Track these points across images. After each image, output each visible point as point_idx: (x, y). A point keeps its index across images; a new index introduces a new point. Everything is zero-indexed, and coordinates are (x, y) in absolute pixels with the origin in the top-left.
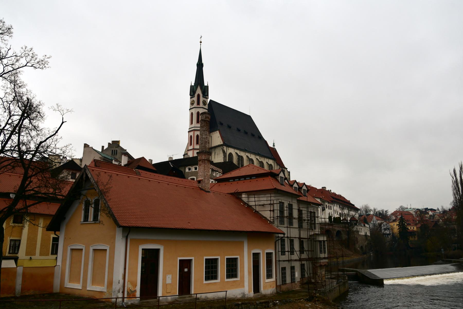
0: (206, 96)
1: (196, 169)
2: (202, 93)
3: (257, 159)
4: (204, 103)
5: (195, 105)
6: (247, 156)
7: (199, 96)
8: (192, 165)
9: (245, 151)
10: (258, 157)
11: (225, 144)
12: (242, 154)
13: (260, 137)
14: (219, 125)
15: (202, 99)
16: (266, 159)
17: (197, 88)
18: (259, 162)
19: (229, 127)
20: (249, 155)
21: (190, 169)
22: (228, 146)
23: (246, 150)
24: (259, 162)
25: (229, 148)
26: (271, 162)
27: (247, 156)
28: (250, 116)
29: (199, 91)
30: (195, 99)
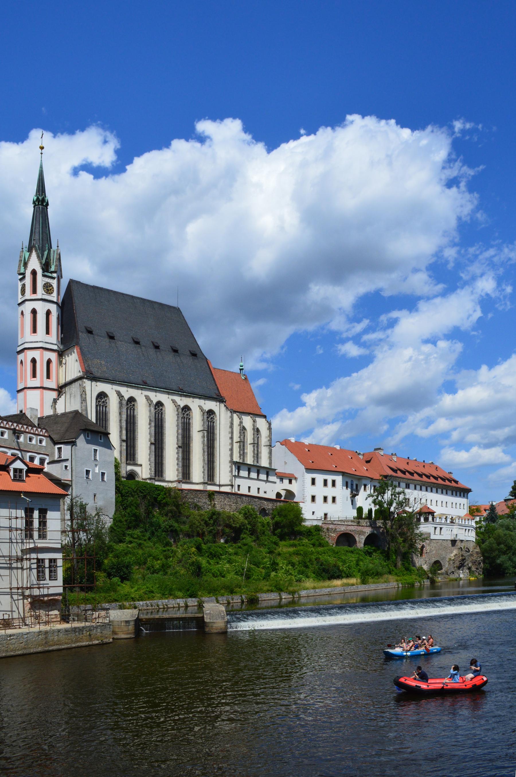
3: (174, 401)
5: (28, 294)
19: (112, 338)
23: (145, 383)
24: (177, 406)
28: (176, 311)
30: (28, 281)
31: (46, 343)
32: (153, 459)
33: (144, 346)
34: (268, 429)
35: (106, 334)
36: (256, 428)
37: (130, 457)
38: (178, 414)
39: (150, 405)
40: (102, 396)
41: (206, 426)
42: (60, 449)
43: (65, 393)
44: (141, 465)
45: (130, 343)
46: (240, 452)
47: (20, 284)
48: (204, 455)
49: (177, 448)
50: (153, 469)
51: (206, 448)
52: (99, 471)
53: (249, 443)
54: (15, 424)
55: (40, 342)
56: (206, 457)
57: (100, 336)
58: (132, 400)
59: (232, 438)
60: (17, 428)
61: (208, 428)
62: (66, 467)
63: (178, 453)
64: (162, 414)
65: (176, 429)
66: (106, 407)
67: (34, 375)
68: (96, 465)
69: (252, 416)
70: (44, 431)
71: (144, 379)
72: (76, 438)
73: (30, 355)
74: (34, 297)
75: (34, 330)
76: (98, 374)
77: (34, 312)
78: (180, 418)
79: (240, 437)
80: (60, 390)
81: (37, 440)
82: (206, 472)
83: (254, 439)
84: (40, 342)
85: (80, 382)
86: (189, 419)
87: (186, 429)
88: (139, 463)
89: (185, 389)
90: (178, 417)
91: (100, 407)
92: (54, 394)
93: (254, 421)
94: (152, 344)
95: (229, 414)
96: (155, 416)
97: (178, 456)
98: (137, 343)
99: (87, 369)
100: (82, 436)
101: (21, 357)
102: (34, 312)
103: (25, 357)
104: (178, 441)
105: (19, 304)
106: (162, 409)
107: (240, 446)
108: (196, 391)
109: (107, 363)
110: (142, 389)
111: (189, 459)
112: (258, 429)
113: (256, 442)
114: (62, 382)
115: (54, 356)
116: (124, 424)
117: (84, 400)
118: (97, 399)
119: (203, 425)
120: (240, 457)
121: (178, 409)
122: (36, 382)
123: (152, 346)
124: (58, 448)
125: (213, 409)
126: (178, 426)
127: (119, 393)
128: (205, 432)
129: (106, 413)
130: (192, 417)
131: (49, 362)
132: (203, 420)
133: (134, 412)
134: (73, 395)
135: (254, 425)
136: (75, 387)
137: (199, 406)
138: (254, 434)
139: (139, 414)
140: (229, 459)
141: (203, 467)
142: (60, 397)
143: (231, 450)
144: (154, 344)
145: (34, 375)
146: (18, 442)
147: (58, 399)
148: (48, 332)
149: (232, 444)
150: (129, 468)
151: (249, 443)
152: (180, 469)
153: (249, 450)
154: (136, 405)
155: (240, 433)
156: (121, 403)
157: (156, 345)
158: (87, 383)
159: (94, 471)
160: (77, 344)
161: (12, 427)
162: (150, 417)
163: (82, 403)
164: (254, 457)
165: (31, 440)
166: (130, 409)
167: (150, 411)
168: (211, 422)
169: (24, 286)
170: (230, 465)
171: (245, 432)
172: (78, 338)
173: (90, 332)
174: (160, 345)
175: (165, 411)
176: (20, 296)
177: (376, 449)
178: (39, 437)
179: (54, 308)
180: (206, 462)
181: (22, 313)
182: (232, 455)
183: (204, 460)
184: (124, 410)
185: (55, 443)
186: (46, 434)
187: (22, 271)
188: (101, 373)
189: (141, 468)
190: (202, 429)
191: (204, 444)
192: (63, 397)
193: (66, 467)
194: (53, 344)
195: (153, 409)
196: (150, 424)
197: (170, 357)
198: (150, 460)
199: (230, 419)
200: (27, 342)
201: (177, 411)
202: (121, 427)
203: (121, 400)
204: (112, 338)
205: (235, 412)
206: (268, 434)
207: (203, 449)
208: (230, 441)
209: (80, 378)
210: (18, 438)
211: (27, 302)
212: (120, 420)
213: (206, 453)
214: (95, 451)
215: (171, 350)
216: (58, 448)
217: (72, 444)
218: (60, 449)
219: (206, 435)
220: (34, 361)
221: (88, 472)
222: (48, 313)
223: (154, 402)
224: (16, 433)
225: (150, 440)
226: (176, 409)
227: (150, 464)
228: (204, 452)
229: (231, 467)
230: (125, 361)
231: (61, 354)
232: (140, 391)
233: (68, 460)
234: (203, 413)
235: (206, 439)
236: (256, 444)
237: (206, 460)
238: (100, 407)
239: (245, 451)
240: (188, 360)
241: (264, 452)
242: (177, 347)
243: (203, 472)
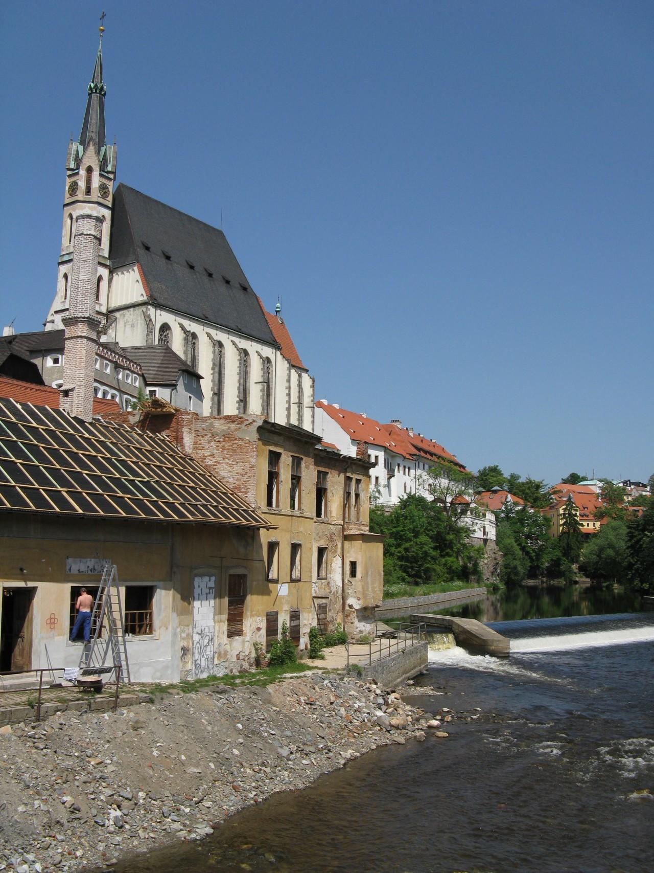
10: (237, 340)
11: (154, 301)
13: (245, 288)
14: (141, 251)
15: (96, 181)
17: (85, 149)
19: (168, 258)
21: (56, 361)
22: (158, 306)
25: (163, 313)
26: (268, 351)
28: (220, 234)
40: (165, 328)
47: (68, 181)
59: (289, 395)
74: (88, 198)
76: (161, 301)
85: (144, 308)
89: (243, 330)
95: (286, 365)
98: (192, 267)
105: (65, 205)
108: (253, 333)
143: (288, 409)
158: (152, 311)
163: (148, 335)
173: (147, 248)
176: (67, 195)
177: (393, 421)
179: (107, 213)
190: (261, 380)
196: (213, 369)
197: (223, 289)
204: (168, 258)
205: (293, 366)
208: (287, 398)
232: (202, 327)
240: (239, 294)
241: (307, 413)
242: (229, 278)
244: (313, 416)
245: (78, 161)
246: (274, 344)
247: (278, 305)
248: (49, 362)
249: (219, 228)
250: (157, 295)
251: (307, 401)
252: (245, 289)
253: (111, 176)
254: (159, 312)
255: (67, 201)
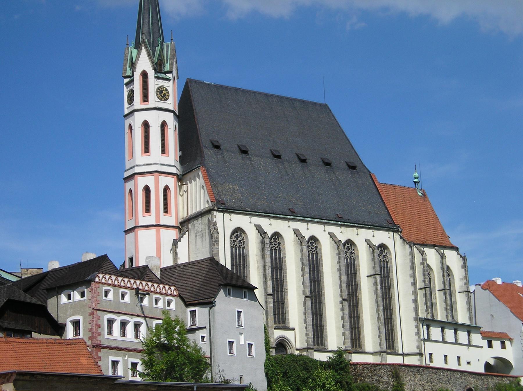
0: (166, 73)
1: (83, 295)
2: (155, 69)
4: (162, 94)
6: (297, 232)
7: (145, 75)
8: (73, 286)
9: (290, 214)
10: (336, 230)
12: (271, 226)
15: (153, 84)
16: (362, 231)
17: (139, 54)
18: (337, 242)
20: (302, 227)
21: (69, 298)
24: (337, 242)
26: (380, 237)
27: (297, 232)
28: (324, 107)
29: (144, 63)
31: (162, 165)
32: (310, 320)
33: (287, 161)
34: (462, 268)
35: (238, 149)
36: (445, 266)
37: (279, 318)
38: (339, 254)
39: (301, 242)
41: (378, 268)
42: (193, 313)
43: (188, 231)
44: (294, 329)
45: (268, 158)
46: (426, 304)
48: (378, 311)
49: (341, 303)
50: (311, 335)
51: (380, 300)
52: (245, 342)
53: (437, 288)
54: (138, 282)
55: (154, 164)
56: (381, 313)
57: (231, 152)
58: (277, 235)
59: (414, 284)
60: (141, 287)
61: (381, 271)
62: (203, 338)
63: (342, 310)
64: (317, 254)
65: (338, 274)
66: (243, 248)
67: (148, 209)
68: (241, 334)
69: (437, 248)
70: (173, 288)
71: (291, 207)
72: (215, 298)
73: (142, 182)
75: (147, 149)
76: (231, 205)
77: (146, 125)
78: (343, 259)
79: (424, 281)
80: (183, 226)
81: (164, 302)
82: (383, 336)
83: (444, 283)
84: (154, 164)
85: (209, 216)
86: (354, 259)
87: (351, 273)
88: (291, 326)
90: (339, 258)
91: (236, 249)
92: (173, 234)
93: (442, 256)
94: (296, 156)
96: (309, 257)
97: (343, 314)
99: (217, 198)
100: (222, 293)
101: (129, 185)
102: (146, 125)
103: (136, 185)
104: (341, 292)
105: (125, 116)
106: (316, 247)
107: (426, 294)
109: (242, 187)
110: (289, 220)
111: (358, 318)
112: (448, 267)
113: (447, 287)
114: (183, 215)
115: (171, 182)
116: (269, 272)
117: (214, 240)
118: (231, 238)
119: (374, 267)
120: (427, 310)
121: (338, 246)
122: (151, 219)
123: (297, 159)
124: (190, 311)
125: (385, 243)
126: (340, 270)
127: (259, 228)
128: (378, 277)
129: (243, 256)
130: (358, 256)
131: (166, 189)
132: (373, 260)
133: (280, 254)
134: (200, 233)
135: (442, 263)
136: (200, 225)
137: (366, 240)
138: (443, 276)
139: (286, 256)
140: (414, 315)
141: (379, 328)
142: (182, 237)
144: (299, 157)
145: (148, 209)
146: (141, 306)
147: (180, 240)
148: (163, 151)
149: (415, 293)
150: (278, 334)
151: (437, 288)
152: (348, 333)
153: (439, 298)
154: (282, 244)
155: (424, 275)
156: (263, 243)
157: (302, 158)
159: (238, 341)
160: (203, 164)
161: (135, 286)
162: (302, 259)
164: (446, 309)
165: (157, 301)
166: (276, 250)
167: (302, 251)
168: (383, 262)
169: (131, 92)
170: (415, 323)
171: (431, 273)
172: (202, 155)
173: (217, 147)
174: (308, 157)
175: (321, 249)
176: (126, 105)
178: (167, 298)
180: (382, 321)
181: (130, 126)
182: (416, 309)
183: (379, 318)
184: (268, 253)
185: (187, 305)
186: (175, 293)
187: (129, 73)
188: (235, 202)
189: (293, 332)
190: (372, 272)
191: (377, 295)
192: (186, 237)
193: (203, 338)
194: (170, 166)
195: (305, 248)
196: (303, 270)
197: (321, 173)
198: (305, 321)
199: (410, 257)
200: (137, 166)
201: (338, 248)
202: (265, 277)
203: (263, 238)
204: (245, 152)
206: (464, 274)
207: (377, 302)
208: (412, 289)
209: (209, 211)
210: (141, 300)
211: (136, 113)
212: (264, 267)
213: (381, 308)
214: (239, 313)
215: (321, 163)
216: (190, 311)
217: (211, 306)
218: (193, 313)
219: (378, 280)
220: (147, 190)
221: (231, 343)
222: (164, 125)
223: (307, 238)
224: (140, 294)
225: (304, 292)
226: (336, 247)
227: (306, 328)
228: (378, 306)
229: (417, 326)
230: (264, 183)
231: (181, 179)
233: (205, 328)
234: (373, 250)
235: (379, 287)
236: (448, 290)
237: (382, 317)
238: (236, 249)
239: (434, 301)
240: (345, 176)
241: (460, 301)
242: (329, 157)
243: (379, 336)
244: (469, 302)
245: (133, 66)
246: (391, 227)
247: (416, 175)
248: (63, 299)
249: (322, 102)
250: (226, 198)
251: (458, 284)
252: (353, 167)
253: (170, 76)
254: (227, 215)
255: (126, 112)
